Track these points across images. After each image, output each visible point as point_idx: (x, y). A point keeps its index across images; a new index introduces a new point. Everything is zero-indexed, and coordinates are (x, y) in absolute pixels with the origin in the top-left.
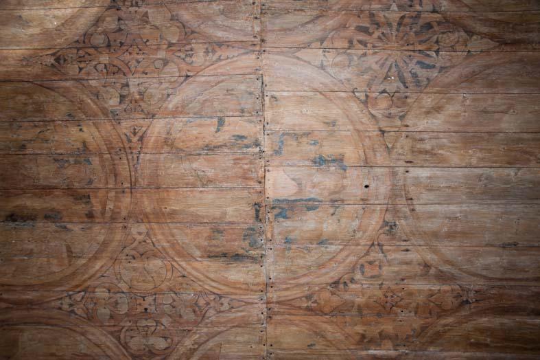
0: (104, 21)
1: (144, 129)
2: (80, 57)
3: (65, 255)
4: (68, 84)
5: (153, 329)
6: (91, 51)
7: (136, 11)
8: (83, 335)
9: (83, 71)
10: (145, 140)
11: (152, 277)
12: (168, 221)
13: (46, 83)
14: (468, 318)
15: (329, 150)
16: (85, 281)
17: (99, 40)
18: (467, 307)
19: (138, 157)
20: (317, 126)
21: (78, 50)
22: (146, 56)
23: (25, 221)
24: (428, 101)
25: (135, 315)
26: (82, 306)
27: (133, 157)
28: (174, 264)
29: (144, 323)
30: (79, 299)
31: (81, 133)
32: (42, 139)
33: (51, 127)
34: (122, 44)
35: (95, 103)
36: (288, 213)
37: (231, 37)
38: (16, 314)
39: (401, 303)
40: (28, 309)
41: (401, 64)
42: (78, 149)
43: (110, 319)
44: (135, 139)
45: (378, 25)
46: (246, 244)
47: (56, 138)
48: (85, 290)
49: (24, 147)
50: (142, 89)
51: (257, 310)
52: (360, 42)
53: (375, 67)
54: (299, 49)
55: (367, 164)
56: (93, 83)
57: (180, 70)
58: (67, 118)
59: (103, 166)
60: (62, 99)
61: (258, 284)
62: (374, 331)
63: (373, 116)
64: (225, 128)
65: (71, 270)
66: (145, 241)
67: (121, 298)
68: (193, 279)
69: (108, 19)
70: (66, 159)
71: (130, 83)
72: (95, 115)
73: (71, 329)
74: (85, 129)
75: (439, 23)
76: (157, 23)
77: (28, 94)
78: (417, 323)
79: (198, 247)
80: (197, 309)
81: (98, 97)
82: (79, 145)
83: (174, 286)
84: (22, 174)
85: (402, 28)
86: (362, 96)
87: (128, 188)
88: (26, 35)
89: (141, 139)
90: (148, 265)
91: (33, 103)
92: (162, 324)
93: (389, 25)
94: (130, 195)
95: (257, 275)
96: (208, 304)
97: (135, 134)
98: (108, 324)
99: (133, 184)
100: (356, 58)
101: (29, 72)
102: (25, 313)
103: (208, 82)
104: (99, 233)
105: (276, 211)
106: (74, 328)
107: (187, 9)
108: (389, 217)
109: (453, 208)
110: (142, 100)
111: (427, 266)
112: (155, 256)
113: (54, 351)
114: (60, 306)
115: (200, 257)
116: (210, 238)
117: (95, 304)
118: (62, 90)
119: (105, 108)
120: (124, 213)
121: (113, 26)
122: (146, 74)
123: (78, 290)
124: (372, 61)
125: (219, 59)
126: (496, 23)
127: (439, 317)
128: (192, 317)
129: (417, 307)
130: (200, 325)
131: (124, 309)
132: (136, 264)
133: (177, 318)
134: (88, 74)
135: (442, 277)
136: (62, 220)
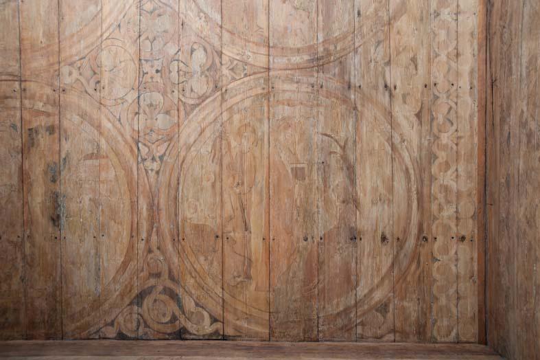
3: (96, 162)
5: (181, 65)
8: (190, 148)
11: (120, 62)
12: (57, 41)
16: (126, 141)
23: (59, 206)
25: (164, 84)
26: (154, 146)
28: (105, 36)
30: (147, 149)
38: (165, 225)
40: (159, 210)
43: (170, 115)
48: (137, 143)
65: (112, 155)
66: (79, 68)
67: (144, 100)
68: (122, 15)
73: (183, 161)
80: (157, 12)
83: (131, 38)
87: (20, 85)
90: (106, 66)
92: (176, 54)
94: (27, 83)
98: (176, 118)
99: (16, 79)
102: (163, 214)
104: (71, 120)
106: (181, 159)
113: (209, 184)
114: (154, 172)
115: (97, 6)
117: (151, 130)
120: (48, 91)
123: (136, 151)
130: (177, 10)
131: (158, 98)
136: (57, 161)
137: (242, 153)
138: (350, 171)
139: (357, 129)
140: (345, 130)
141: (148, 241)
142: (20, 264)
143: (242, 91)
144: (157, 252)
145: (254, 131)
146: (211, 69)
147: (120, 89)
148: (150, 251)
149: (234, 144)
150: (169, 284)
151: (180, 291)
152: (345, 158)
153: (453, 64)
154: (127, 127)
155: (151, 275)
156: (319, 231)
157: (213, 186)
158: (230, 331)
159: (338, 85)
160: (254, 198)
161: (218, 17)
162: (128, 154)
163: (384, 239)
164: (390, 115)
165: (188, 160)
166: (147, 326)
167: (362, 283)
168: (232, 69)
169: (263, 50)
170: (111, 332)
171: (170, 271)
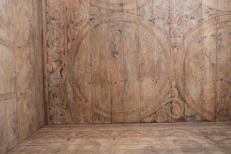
0: (159, 25)
1: (206, 8)
2: (174, 36)
4: (185, 42)
6: (172, 31)
7: (155, 11)
9: (180, 35)
10: (211, 7)
13: (185, 53)
19: (219, 11)
21: (171, 37)
22: (174, 6)
27: (219, 13)
31: (207, 37)
32: (210, 55)
34: (169, 18)
35: (194, 30)
42: (214, 39)
47: (209, 49)
49: (213, 64)
50: (188, 9)
56: (185, 31)
58: (200, 43)
59: (223, 27)
70: (219, 45)
71: (186, 14)
77: (190, 61)
81: (192, 29)
82: (213, 38)
84: (225, 66)
88: (165, 60)
89: (211, 9)
91: (194, 59)
97: (208, 12)
101: (180, 60)
118: (188, 46)
119: (196, 26)
122: (182, 7)
134: (181, 33)
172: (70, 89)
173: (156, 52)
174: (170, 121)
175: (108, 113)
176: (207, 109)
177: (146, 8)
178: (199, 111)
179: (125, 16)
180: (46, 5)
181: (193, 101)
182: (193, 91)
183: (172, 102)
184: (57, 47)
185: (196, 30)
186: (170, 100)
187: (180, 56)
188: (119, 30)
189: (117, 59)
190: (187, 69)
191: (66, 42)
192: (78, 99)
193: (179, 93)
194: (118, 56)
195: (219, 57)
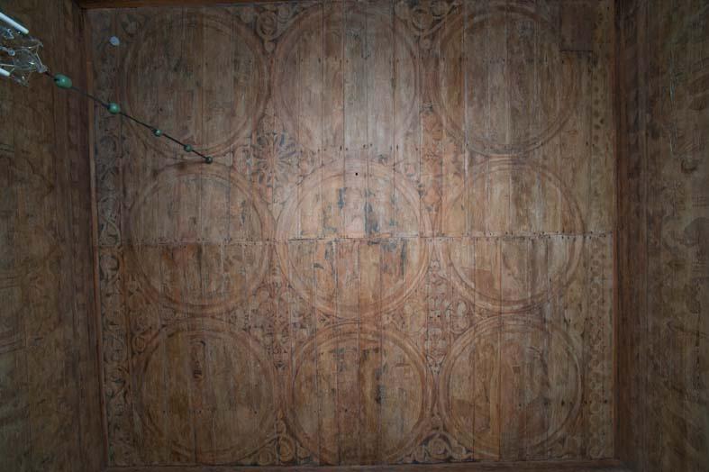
4: (294, 360)
13: (294, 374)
14: (442, 107)
15: (333, 199)
16: (420, 356)
17: (268, 340)
18: (434, 107)
20: (319, 206)
24: (303, 138)
29: (448, 317)
33: (320, 372)
36: (374, 223)
37: (266, 258)
38: (442, 401)
39: (432, 149)
41: (281, 156)
44: (328, 320)
45: (259, 170)
46: (394, 251)
49: (333, 390)
50: (297, 314)
51: (439, 243)
52: (268, 181)
53: (284, 170)
54: (273, 218)
55: (343, 175)
57: (286, 291)
59: (345, 341)
60: (303, 365)
61: (421, 243)
62: (452, 167)
63: (313, 172)
64: (320, 262)
65: (412, 365)
69: (255, 334)
72: (313, 344)
74: (321, 351)
75: (258, 134)
76: (258, 304)
77: (301, 385)
78: (446, 138)
79: (396, 281)
85: (261, 155)
86: (301, 179)
89: (327, 316)
93: (260, 162)
95: (415, 244)
96: (434, 276)
100: (278, 183)
103: (293, 273)
104: (388, 345)
105: (373, 231)
107: (250, 286)
108: (376, 160)
109: (370, 120)
110: (303, 315)
111: (408, 134)
112: (402, 309)
113: (467, 378)
116: (391, 273)
120: (375, 328)
121: (260, 331)
124: (279, 174)
125: (279, 266)
126: (258, 101)
127: (441, 125)
128: (443, 286)
129: (436, 140)
131: (439, 331)
132: (408, 322)
133: (444, 296)
135: (414, 125)
137: (486, 360)
138: (545, 366)
139: (549, 345)
140: (543, 346)
141: (432, 410)
142: (357, 425)
143: (485, 326)
144: (437, 416)
145: (492, 347)
146: (469, 314)
147: (416, 328)
148: (433, 415)
149: (481, 355)
150: (443, 433)
151: (449, 437)
152: (542, 360)
153: (601, 307)
154: (421, 348)
155: (434, 429)
156: (528, 400)
157: (470, 378)
158: (477, 457)
159: (540, 321)
160: (492, 384)
161: (473, 286)
162: (421, 363)
163: (563, 403)
164: (566, 336)
165: (456, 365)
166: (430, 456)
167: (551, 428)
168: (480, 314)
169: (498, 303)
170: (409, 460)
171: (444, 426)
172: (137, 419)
173: (253, 373)
174: (277, 463)
175: (190, 451)
176: (328, 449)
177: (239, 313)
178: (317, 452)
179: (208, 322)
180: (102, 304)
181: (308, 438)
182: (308, 426)
183: (278, 438)
184: (118, 362)
185: (307, 346)
186: (276, 436)
187: (286, 378)
188: (202, 342)
189: (200, 381)
190: (297, 395)
191: (130, 356)
192: (148, 432)
193: (288, 427)
194: (202, 377)
195: (341, 380)
